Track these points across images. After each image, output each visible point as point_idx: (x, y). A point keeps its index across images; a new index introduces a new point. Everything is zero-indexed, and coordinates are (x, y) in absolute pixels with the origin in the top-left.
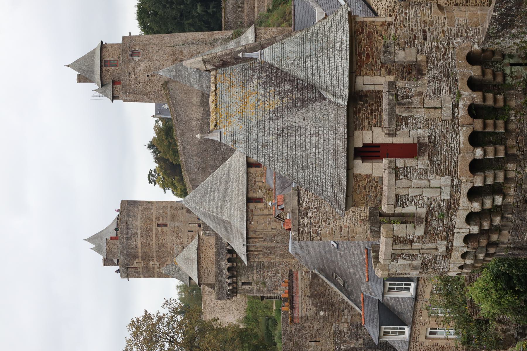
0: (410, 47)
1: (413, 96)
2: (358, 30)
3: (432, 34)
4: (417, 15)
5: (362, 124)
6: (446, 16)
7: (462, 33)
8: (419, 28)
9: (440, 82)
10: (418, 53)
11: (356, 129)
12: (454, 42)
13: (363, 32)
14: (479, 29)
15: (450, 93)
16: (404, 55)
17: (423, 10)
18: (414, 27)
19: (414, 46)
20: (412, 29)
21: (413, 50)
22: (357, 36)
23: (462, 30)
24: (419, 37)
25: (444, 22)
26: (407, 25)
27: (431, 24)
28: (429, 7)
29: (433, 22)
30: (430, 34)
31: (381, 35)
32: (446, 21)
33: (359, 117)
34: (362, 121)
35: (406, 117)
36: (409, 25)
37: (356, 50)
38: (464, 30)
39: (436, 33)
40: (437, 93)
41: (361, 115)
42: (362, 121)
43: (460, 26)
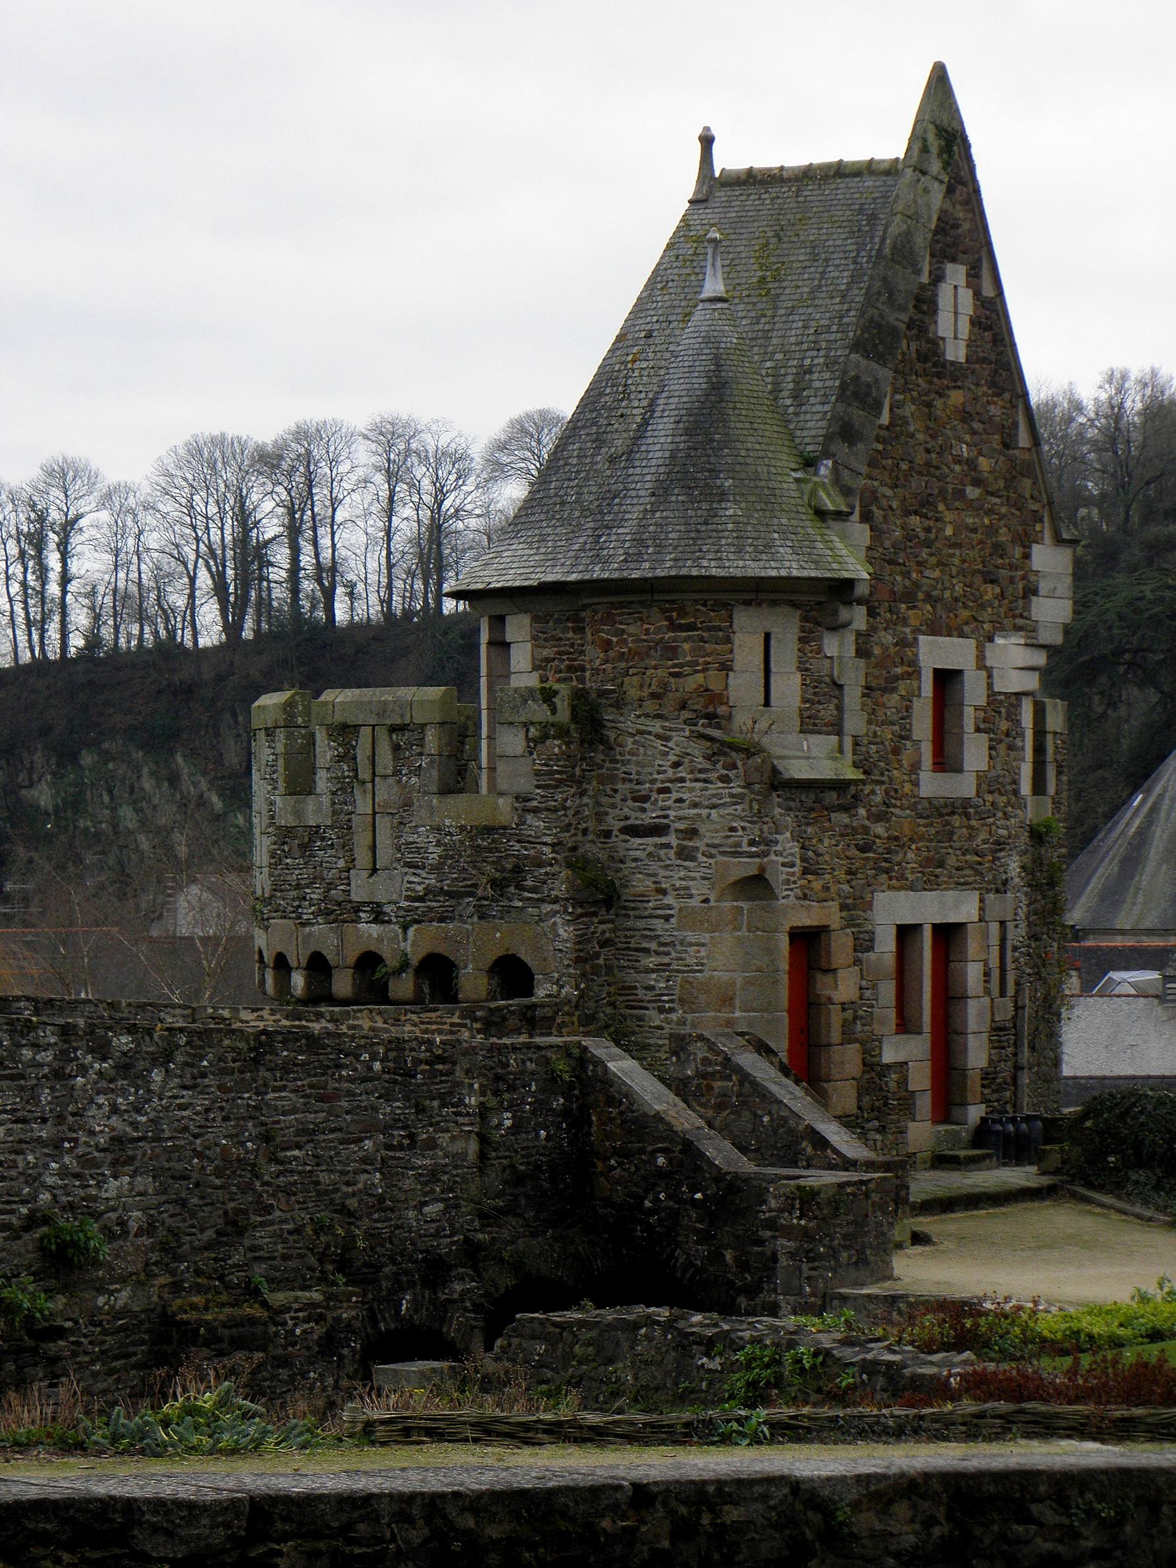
0: (537, 773)
1: (400, 781)
2: (682, 612)
3: (650, 855)
4: (714, 807)
5: (546, 640)
6: (712, 904)
7: (657, 953)
8: (672, 813)
9: (437, 868)
10: (517, 798)
11: (535, 619)
12: (558, 919)
13: (673, 627)
14: (672, 1010)
15: (408, 898)
16: (510, 752)
17: (733, 829)
18: (675, 795)
19: (538, 787)
20: (666, 790)
21: (525, 784)
22: (664, 611)
23: (668, 954)
24: (644, 810)
25: (691, 896)
26: (682, 772)
27: (685, 854)
28: (745, 848)
29: (693, 859)
30: (650, 849)
31: (665, 686)
32: (695, 902)
33: (566, 630)
34: (553, 638)
35: (355, 759)
36: (682, 780)
37: (621, 605)
38: (666, 960)
39: (654, 867)
40: (409, 857)
41: (571, 634)
42: (553, 638)
43: (679, 948)
